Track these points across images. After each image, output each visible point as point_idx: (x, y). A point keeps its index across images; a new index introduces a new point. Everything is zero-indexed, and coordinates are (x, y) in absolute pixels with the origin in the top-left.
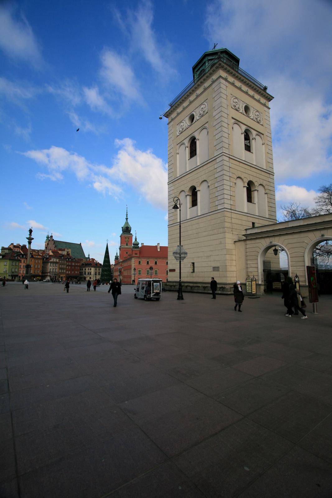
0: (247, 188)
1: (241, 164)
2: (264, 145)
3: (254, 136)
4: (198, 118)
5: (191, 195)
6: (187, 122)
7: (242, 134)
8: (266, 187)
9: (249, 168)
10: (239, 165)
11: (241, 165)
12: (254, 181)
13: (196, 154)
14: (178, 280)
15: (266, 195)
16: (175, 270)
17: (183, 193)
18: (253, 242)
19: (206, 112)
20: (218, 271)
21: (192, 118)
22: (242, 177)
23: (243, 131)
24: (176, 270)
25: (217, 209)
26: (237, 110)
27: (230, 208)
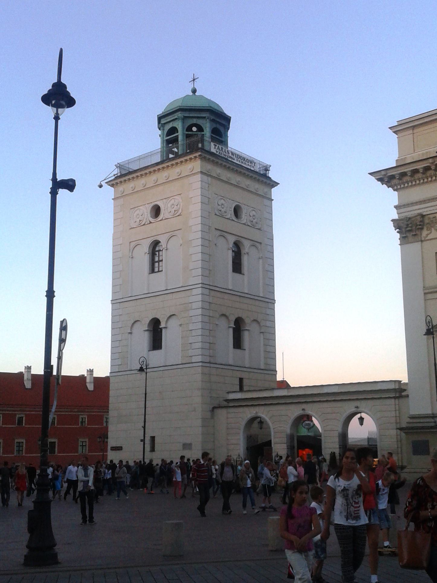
2: (261, 261)
3: (246, 250)
4: (167, 215)
5: (152, 329)
6: (146, 211)
9: (238, 299)
11: (226, 296)
12: (244, 317)
15: (262, 335)
16: (122, 447)
17: (137, 325)
19: (177, 214)
20: (190, 449)
21: (156, 211)
22: (227, 314)
25: (190, 362)
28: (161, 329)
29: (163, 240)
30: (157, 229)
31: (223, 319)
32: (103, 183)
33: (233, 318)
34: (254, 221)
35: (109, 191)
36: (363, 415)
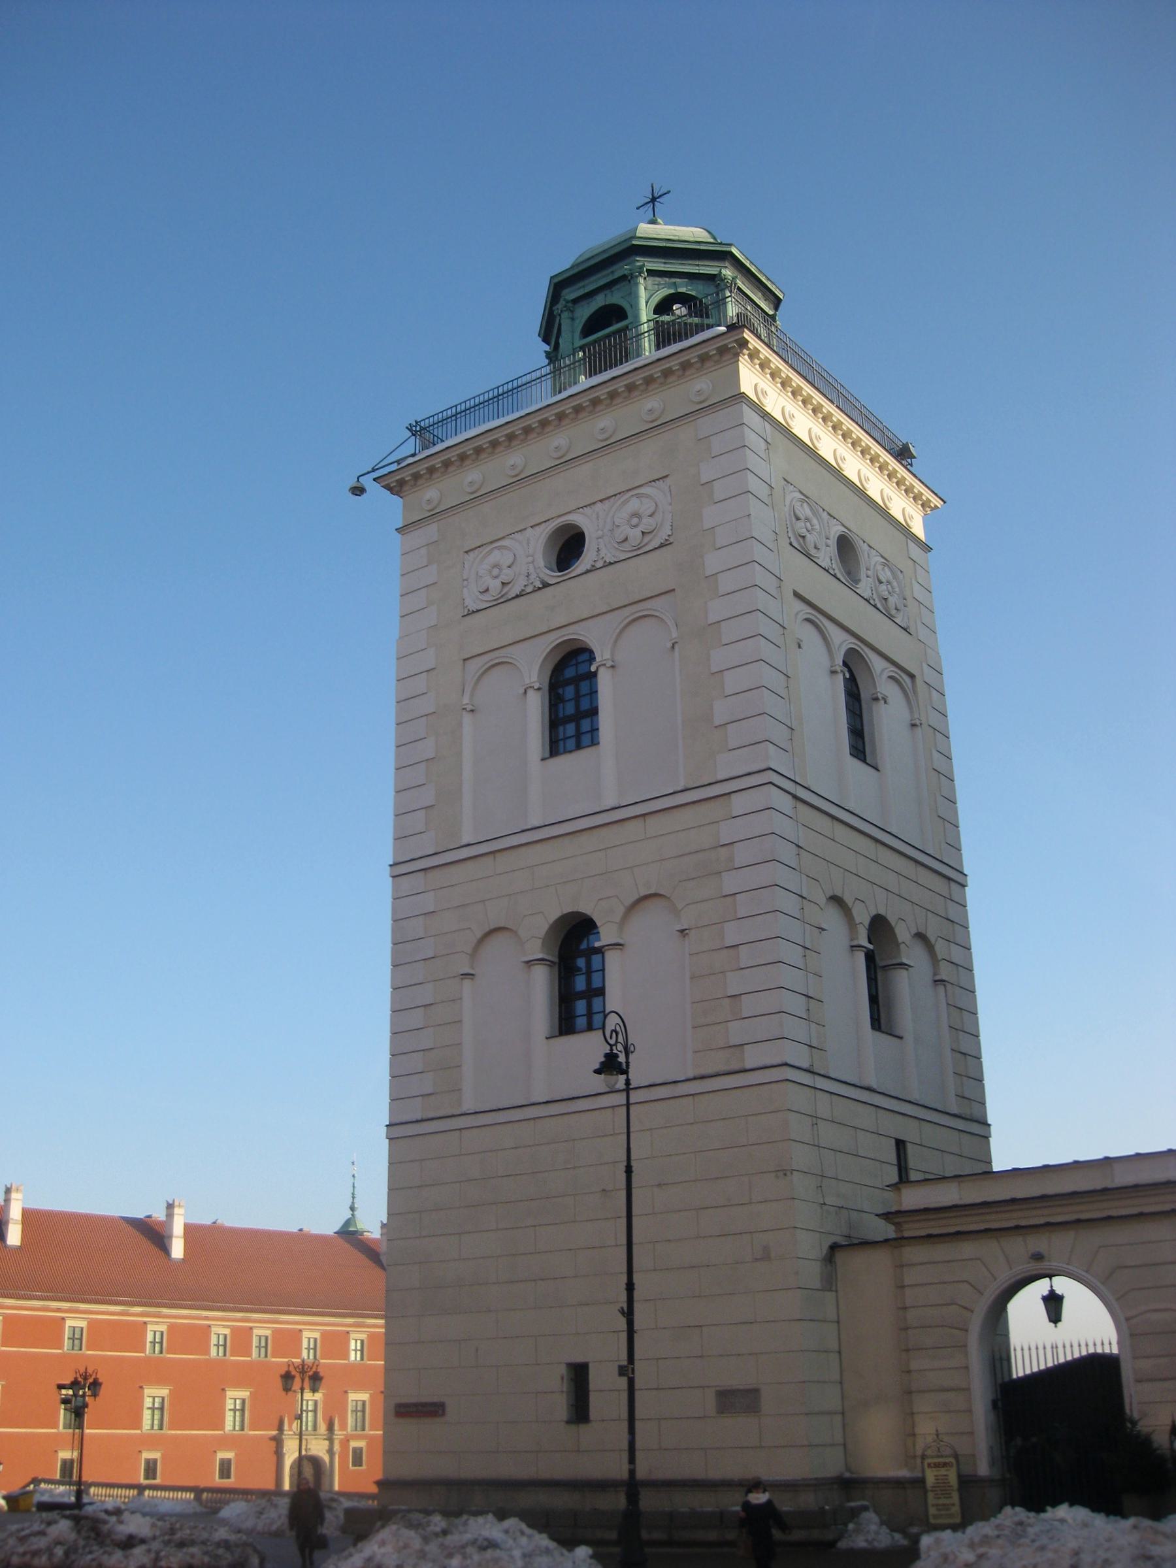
0: (870, 957)
1: (839, 828)
2: (919, 730)
5: (556, 960)
7: (834, 672)
8: (940, 947)
10: (913, 877)
11: (841, 832)
12: (892, 919)
13: (594, 742)
14: (617, 1469)
15: (941, 989)
17: (497, 944)
18: (941, 1252)
19: (656, 543)
21: (568, 547)
23: (839, 661)
24: (448, 1410)
25: (736, 1067)
26: (808, 556)
27: (805, 1065)
28: (600, 951)
29: (594, 636)
30: (576, 606)
31: (832, 919)
32: (367, 482)
33: (863, 917)
34: (892, 601)
35: (388, 508)
36: (1062, 1285)
